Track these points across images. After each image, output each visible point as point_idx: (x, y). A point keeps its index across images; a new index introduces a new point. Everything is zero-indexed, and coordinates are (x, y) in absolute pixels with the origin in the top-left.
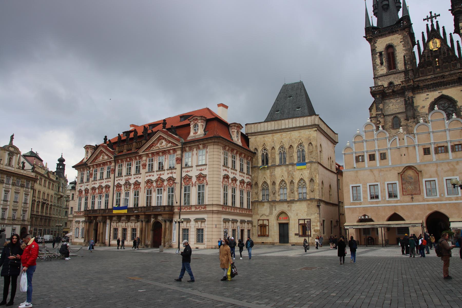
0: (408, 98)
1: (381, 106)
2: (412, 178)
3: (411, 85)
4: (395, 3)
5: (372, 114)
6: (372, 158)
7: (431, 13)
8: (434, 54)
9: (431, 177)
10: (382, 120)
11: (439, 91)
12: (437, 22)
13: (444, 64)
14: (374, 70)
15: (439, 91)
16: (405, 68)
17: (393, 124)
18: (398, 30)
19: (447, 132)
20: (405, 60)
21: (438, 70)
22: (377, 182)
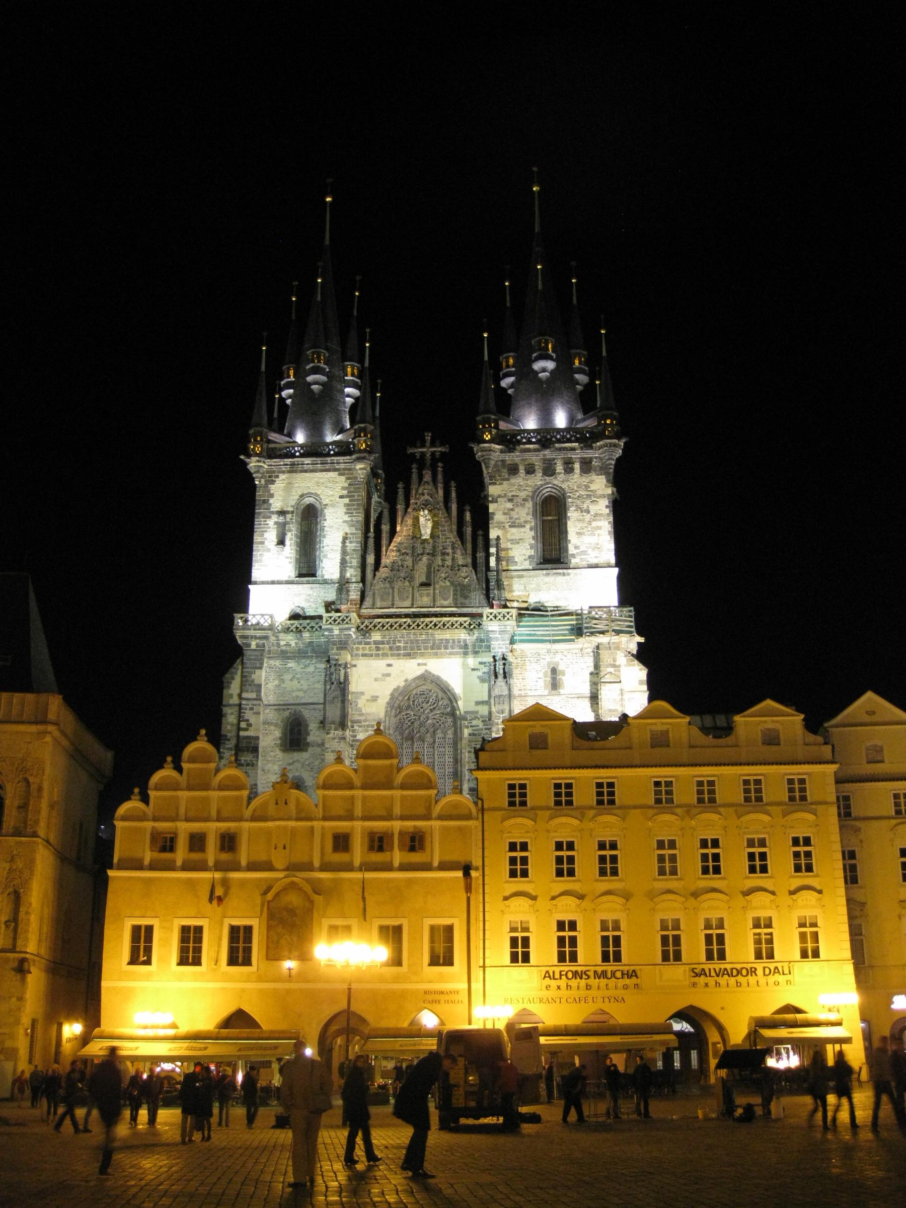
5: (231, 696)
6: (197, 842)
15: (420, 661)
17: (284, 734)
20: (344, 552)
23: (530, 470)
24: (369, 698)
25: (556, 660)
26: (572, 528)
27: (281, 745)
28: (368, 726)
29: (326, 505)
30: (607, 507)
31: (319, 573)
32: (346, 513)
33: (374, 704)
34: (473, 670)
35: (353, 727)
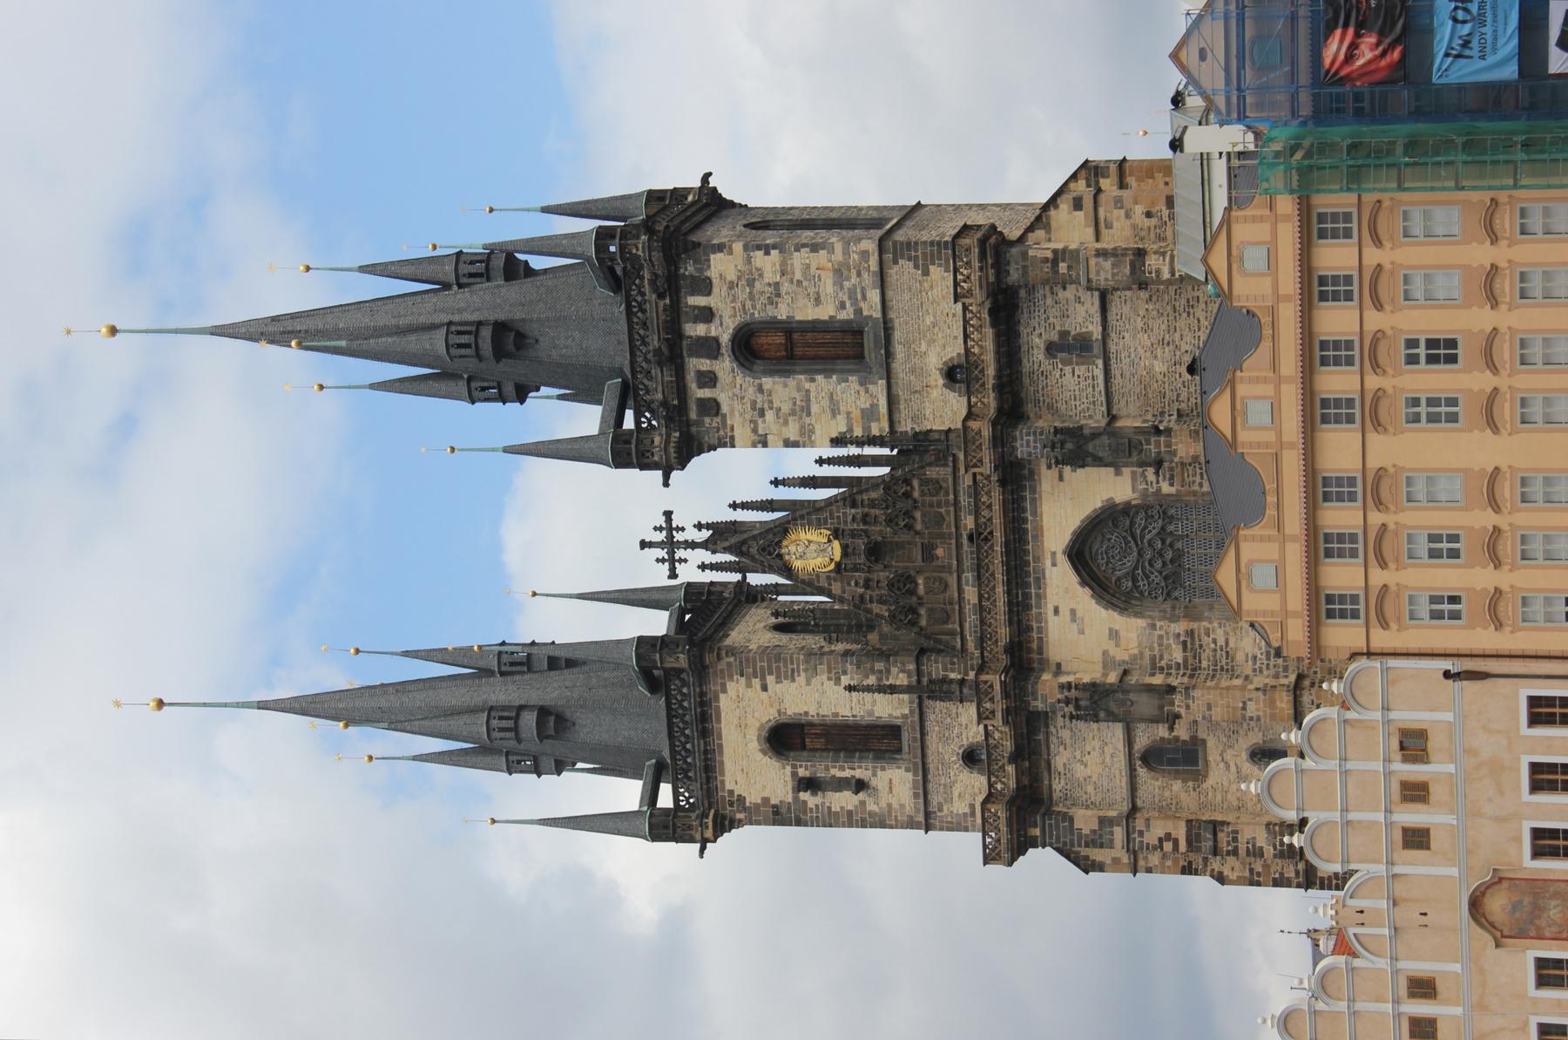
0: (1067, 701)
1: (1085, 821)
2: (1520, 902)
3: (1003, 684)
4: (530, 670)
5: (1116, 861)
7: (644, 545)
8: (862, 559)
9: (1518, 840)
10: (1158, 830)
11: (1048, 562)
12: (699, 526)
13: (919, 527)
14: (883, 825)
15: (1048, 562)
16: (908, 689)
17: (1177, 775)
18: (702, 694)
19: (1350, 765)
20: (868, 689)
21: (940, 552)
22: (1526, 1024)
23: (709, 379)
24: (1112, 643)
25: (1042, 346)
26: (807, 312)
27: (1196, 780)
28: (1160, 645)
29: (779, 711)
30: (767, 253)
31: (899, 722)
32: (793, 680)
33: (1122, 634)
34: (1061, 478)
35: (1162, 669)
